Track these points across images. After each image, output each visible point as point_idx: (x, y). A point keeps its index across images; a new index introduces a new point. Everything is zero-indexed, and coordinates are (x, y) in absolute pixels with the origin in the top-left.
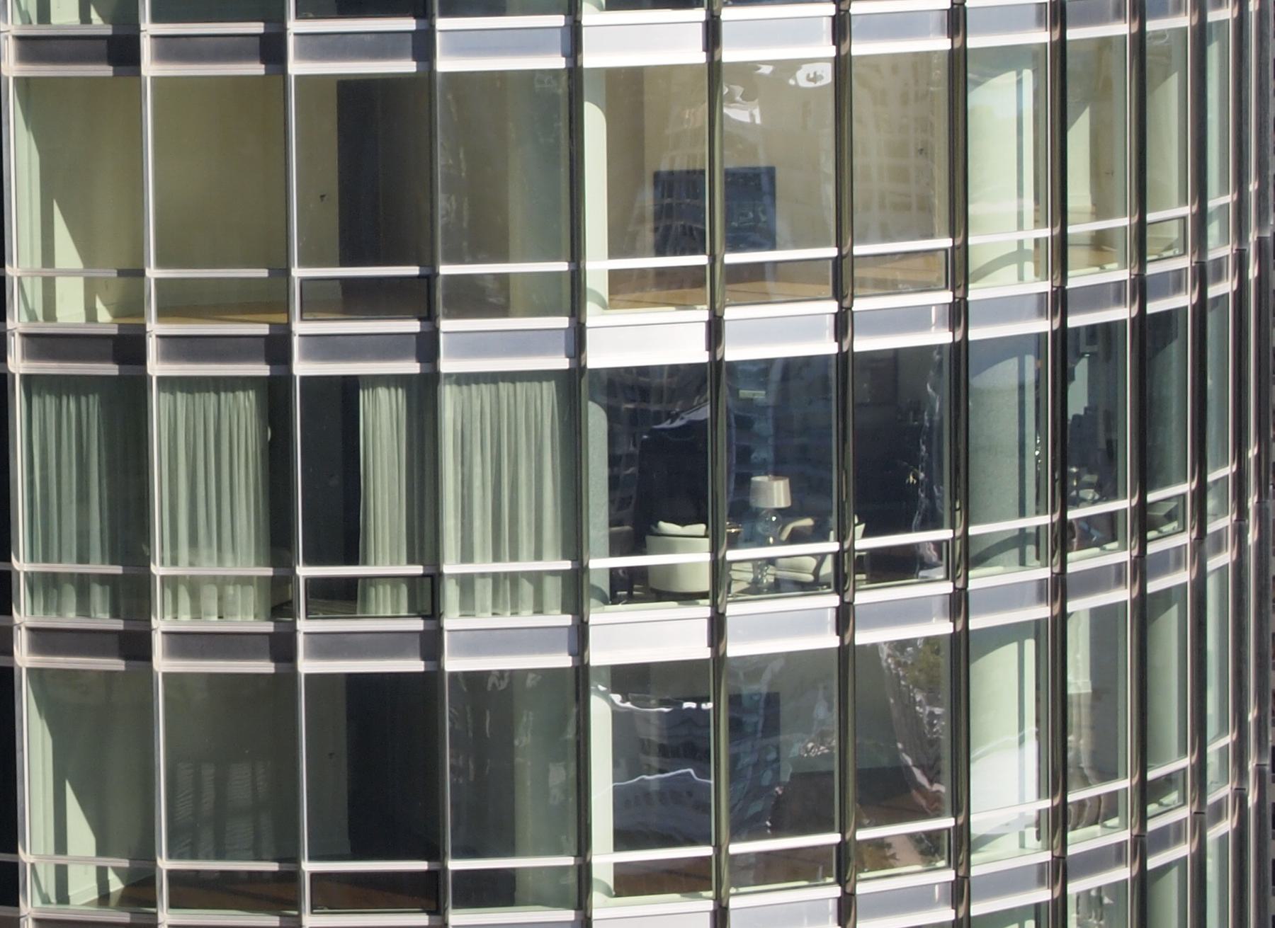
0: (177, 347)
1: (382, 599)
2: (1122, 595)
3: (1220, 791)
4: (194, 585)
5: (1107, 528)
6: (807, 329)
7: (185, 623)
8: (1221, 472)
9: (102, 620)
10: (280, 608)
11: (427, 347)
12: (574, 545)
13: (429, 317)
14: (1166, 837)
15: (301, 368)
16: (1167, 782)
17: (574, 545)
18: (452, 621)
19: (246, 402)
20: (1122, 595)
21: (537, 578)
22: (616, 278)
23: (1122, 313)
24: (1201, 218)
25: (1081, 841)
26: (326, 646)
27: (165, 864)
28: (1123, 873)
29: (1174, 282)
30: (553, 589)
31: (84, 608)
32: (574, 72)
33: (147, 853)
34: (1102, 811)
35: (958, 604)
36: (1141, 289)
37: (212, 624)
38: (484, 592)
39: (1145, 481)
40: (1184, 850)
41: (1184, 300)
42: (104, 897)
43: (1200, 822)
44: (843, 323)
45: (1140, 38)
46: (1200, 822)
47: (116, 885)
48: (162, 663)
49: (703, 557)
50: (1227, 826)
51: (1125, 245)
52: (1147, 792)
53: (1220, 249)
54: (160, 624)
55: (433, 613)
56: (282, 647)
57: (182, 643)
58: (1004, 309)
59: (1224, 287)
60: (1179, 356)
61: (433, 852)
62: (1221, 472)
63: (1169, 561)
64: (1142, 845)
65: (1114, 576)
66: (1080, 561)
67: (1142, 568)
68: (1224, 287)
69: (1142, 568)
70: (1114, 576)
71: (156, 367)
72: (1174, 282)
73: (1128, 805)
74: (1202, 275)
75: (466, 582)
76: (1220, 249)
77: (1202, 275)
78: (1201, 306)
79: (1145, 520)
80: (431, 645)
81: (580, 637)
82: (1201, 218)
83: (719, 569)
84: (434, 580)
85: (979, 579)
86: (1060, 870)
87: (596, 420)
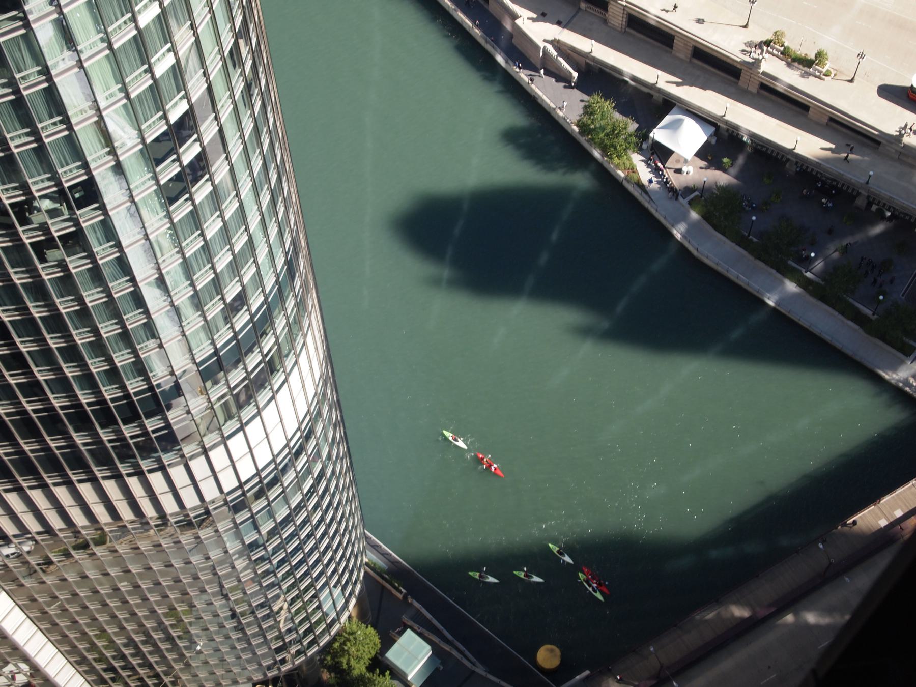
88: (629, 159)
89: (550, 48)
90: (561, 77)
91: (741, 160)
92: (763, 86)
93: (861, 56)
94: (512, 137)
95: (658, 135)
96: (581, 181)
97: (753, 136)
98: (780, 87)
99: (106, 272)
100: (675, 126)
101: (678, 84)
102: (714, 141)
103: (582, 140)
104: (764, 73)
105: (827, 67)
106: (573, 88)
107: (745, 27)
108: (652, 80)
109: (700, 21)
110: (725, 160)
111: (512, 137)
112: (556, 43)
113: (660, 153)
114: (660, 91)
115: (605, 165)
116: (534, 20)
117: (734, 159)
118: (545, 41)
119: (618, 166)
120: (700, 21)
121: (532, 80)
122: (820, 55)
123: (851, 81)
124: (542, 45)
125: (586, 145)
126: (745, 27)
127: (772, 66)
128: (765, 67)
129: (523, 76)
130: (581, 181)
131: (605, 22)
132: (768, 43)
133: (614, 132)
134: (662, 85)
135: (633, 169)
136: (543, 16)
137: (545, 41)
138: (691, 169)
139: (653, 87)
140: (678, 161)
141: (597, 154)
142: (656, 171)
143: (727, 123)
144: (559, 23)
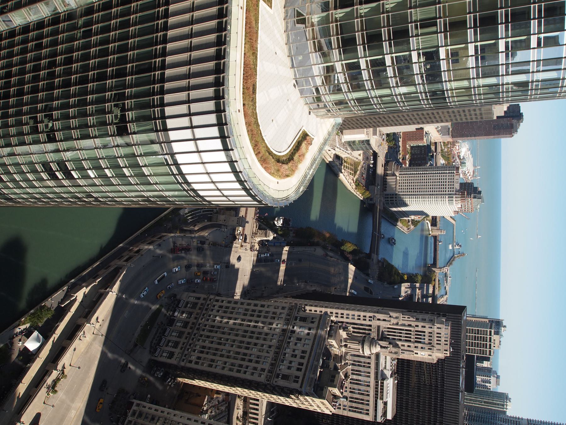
0: (440, 7)
1: (416, 31)
2: (421, 98)
3: (404, 108)
4: (417, 13)
5: (427, 96)
6: (444, 68)
7: (413, 13)
8: (432, 106)
9: (413, 4)
10: (415, 22)
11: (441, 32)
12: (422, 49)
13: (444, 32)
14: (400, 104)
15: (438, 20)
16: (404, 104)
17: (422, 49)
18: (415, 38)
19: (434, 15)
20: (421, 98)
21: (419, 46)
22: (508, 42)
23: (446, 96)
24: (455, 102)
25: (399, 97)
26: (412, 26)
27: (390, 14)
28: (396, 101)
29: (449, 100)
30: (418, 47)
31: (414, 2)
32: (468, 43)
33: (391, 12)
34: (401, 98)
35: (419, 84)
36: (449, 97)
37: (413, 15)
38: (418, 41)
39: (431, 99)
40: (398, 105)
41: (448, 101)
42: (387, 8)
43: (401, 107)
44: (444, 71)
45: (472, 95)
46: (401, 107)
47: (388, 9)
48: (409, 11)
49: (422, 61)
50: (401, 109)
51: (453, 96)
52: (403, 102)
53: (452, 104)
54: (413, 10)
55: (415, 36)
56: (411, 22)
57: (411, 12)
58: (446, 85)
59: (449, 104)
60: (443, 101)
61: (393, 39)
62: (432, 106)
63: (424, 102)
64: (399, 102)
65: (422, 97)
66: (423, 94)
67: (423, 100)
68: (449, 104)
69: (423, 100)
70: (422, 97)
71: (438, 6)
72: (449, 100)
73: (402, 100)
74: (450, 102)
75: (418, 39)
76: (452, 104)
77: (450, 102)
78: (447, 103)
79: (427, 100)
80: (412, 36)
81: (414, 50)
82: (455, 102)
83: (421, 62)
84: (419, 36)
85: (421, 86)
86: (396, 95)
87: (434, 49)
88: (28, 323)
89: (74, 298)
90: (63, 301)
91: (20, 363)
92: (47, 371)
93: (53, 406)
94: (44, 281)
95: (36, 333)
96: (23, 304)
97: (29, 368)
98: (46, 377)
99: (21, 137)
100: (38, 340)
101: (53, 341)
102: (30, 353)
103: (38, 307)
104: (52, 372)
105: (51, 394)
106: (59, 304)
107: (70, 365)
108: (56, 332)
109: (75, 350)
110: (21, 358)
111: (44, 281)
112: (75, 300)
113: (28, 334)
114: (52, 335)
115: (27, 314)
116: (84, 293)
117: (21, 361)
118: (77, 296)
119: (26, 318)
120: (75, 350)
121: (64, 291)
122: (56, 391)
123: (44, 403)
124: (75, 295)
125: (36, 308)
126: (70, 365)
127: (55, 374)
128: (55, 372)
129: (65, 288)
130: (23, 304)
131: (80, 317)
132: (63, 373)
133: (39, 318)
134: (54, 335)
135: (24, 324)
136: (85, 296)
137: (77, 296)
138: (20, 345)
139: (54, 333)
140: (24, 340)
141: (32, 311)
142: (22, 332)
143: (36, 358)
144: (82, 301)
